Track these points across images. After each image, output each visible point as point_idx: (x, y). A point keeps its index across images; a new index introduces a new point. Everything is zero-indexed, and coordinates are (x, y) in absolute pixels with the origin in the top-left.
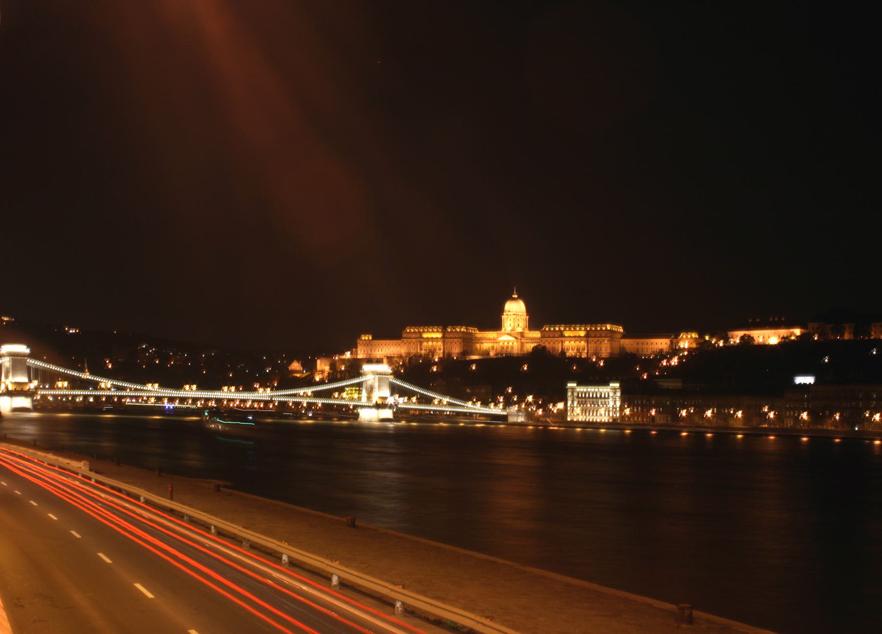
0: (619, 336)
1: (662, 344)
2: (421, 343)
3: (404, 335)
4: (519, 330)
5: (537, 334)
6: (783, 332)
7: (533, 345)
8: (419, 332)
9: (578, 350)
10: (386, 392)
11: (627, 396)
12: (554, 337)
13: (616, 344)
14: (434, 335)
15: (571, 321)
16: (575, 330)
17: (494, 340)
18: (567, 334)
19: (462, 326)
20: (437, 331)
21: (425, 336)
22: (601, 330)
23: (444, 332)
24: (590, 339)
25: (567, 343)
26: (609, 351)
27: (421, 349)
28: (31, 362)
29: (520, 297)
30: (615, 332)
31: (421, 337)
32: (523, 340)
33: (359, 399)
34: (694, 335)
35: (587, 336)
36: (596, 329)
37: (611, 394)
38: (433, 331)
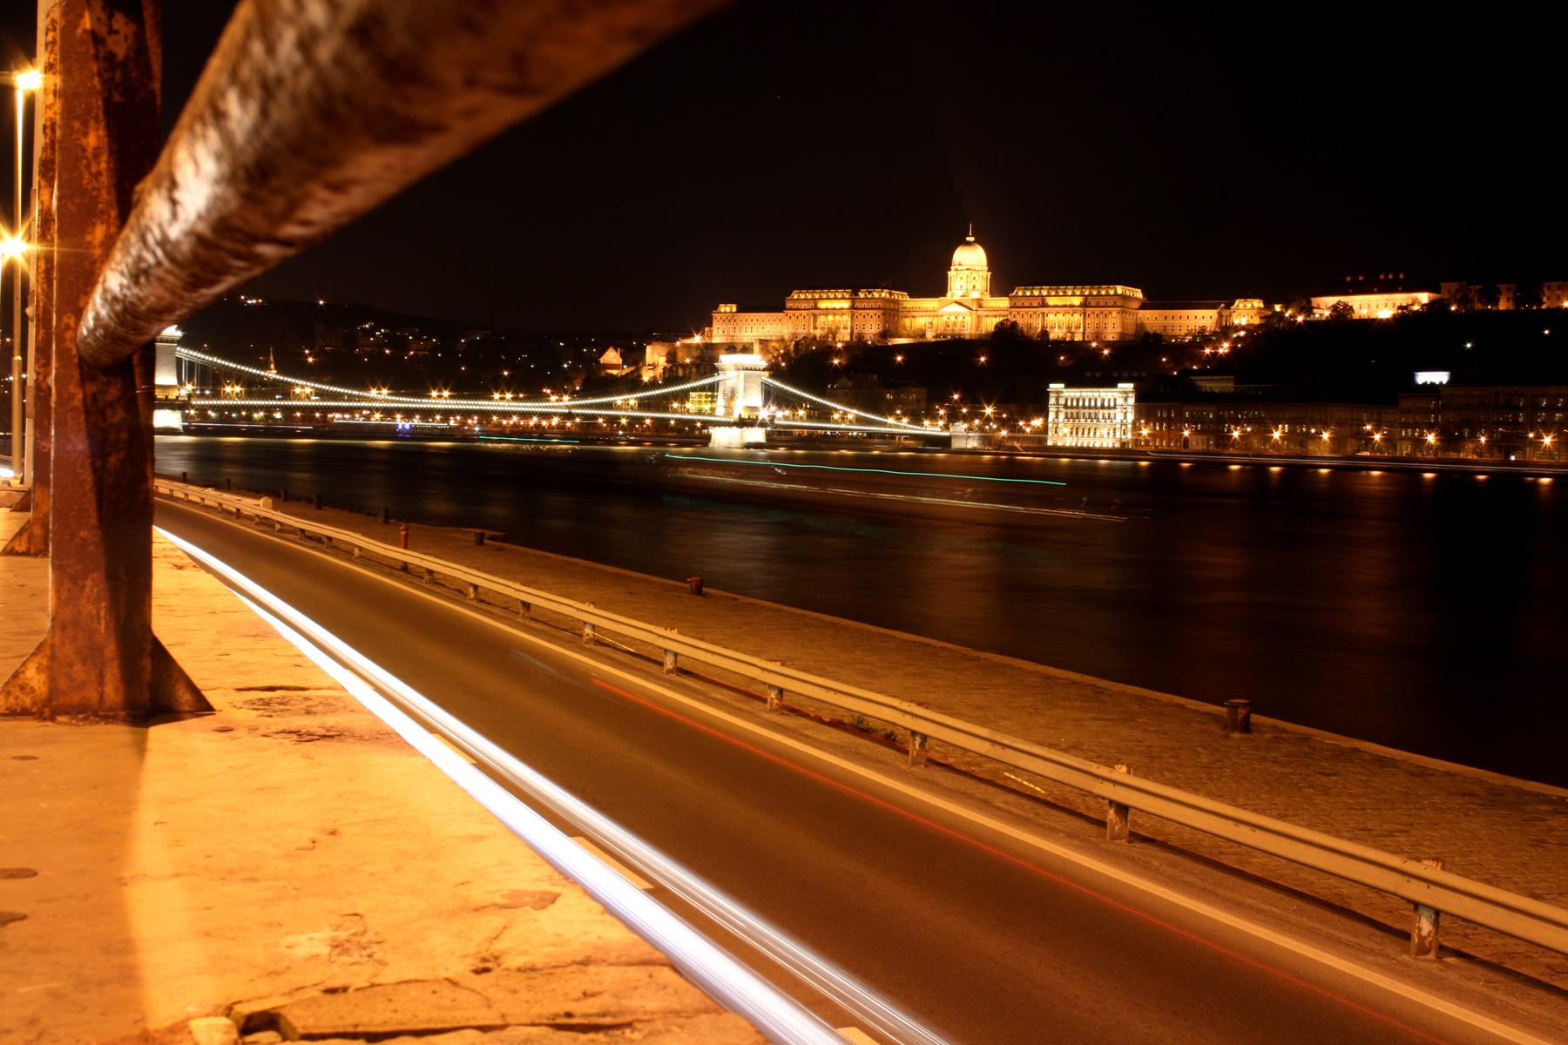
0: (1136, 305)
1: (1204, 318)
3: (789, 305)
4: (976, 295)
5: (1003, 302)
6: (1402, 298)
7: (996, 321)
9: (1069, 328)
10: (756, 398)
11: (1147, 403)
13: (1130, 320)
15: (1059, 278)
17: (934, 313)
18: (1051, 301)
19: (883, 288)
21: (823, 305)
23: (854, 298)
24: (1089, 310)
25: (1051, 317)
26: (1118, 329)
28: (184, 353)
31: (816, 308)
32: (981, 312)
33: (713, 410)
34: (1258, 303)
35: (1085, 305)
36: (1099, 295)
37: (1120, 401)
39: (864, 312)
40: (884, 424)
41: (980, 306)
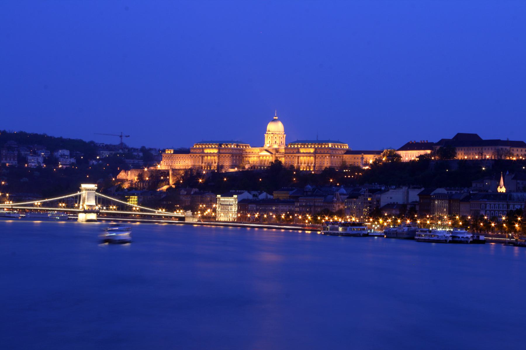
0: (343, 152)
2: (203, 157)
3: (192, 151)
4: (276, 146)
10: (93, 202)
14: (212, 151)
16: (308, 148)
18: (302, 151)
20: (215, 148)
21: (206, 151)
25: (301, 158)
26: (329, 165)
30: (337, 149)
31: (203, 153)
33: (79, 206)
35: (315, 153)
38: (212, 148)
39: (224, 155)
40: (154, 212)
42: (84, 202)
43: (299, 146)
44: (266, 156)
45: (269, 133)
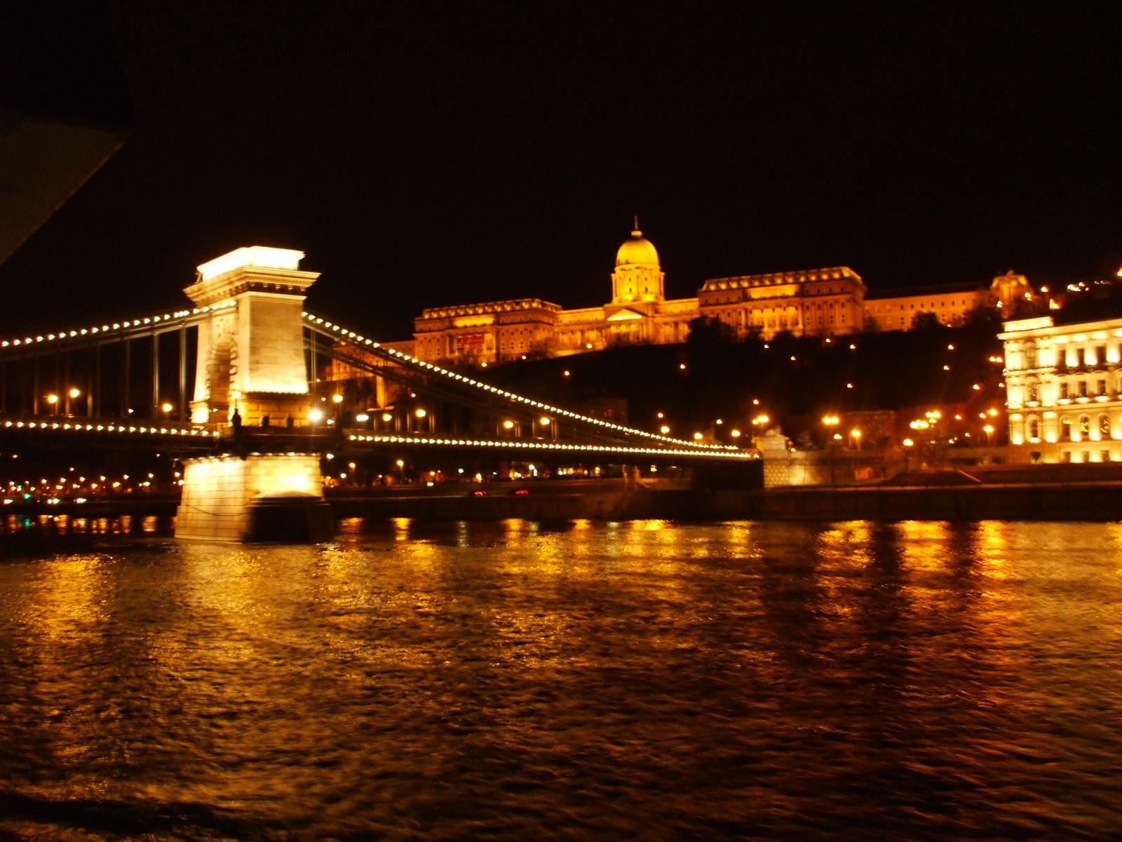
0: (860, 295)
3: (419, 326)
4: (649, 298)
8: (449, 317)
9: (783, 324)
10: (291, 377)
12: (729, 303)
15: (763, 264)
16: (773, 284)
18: (756, 293)
19: (532, 296)
20: (485, 313)
21: (460, 323)
22: (831, 279)
24: (808, 301)
25: (757, 314)
27: (452, 351)
29: (647, 236)
32: (658, 319)
33: (182, 415)
35: (802, 293)
36: (819, 280)
38: (476, 314)
41: (657, 312)
42: (222, 375)
43: (745, 284)
44: (629, 323)
45: (627, 267)
